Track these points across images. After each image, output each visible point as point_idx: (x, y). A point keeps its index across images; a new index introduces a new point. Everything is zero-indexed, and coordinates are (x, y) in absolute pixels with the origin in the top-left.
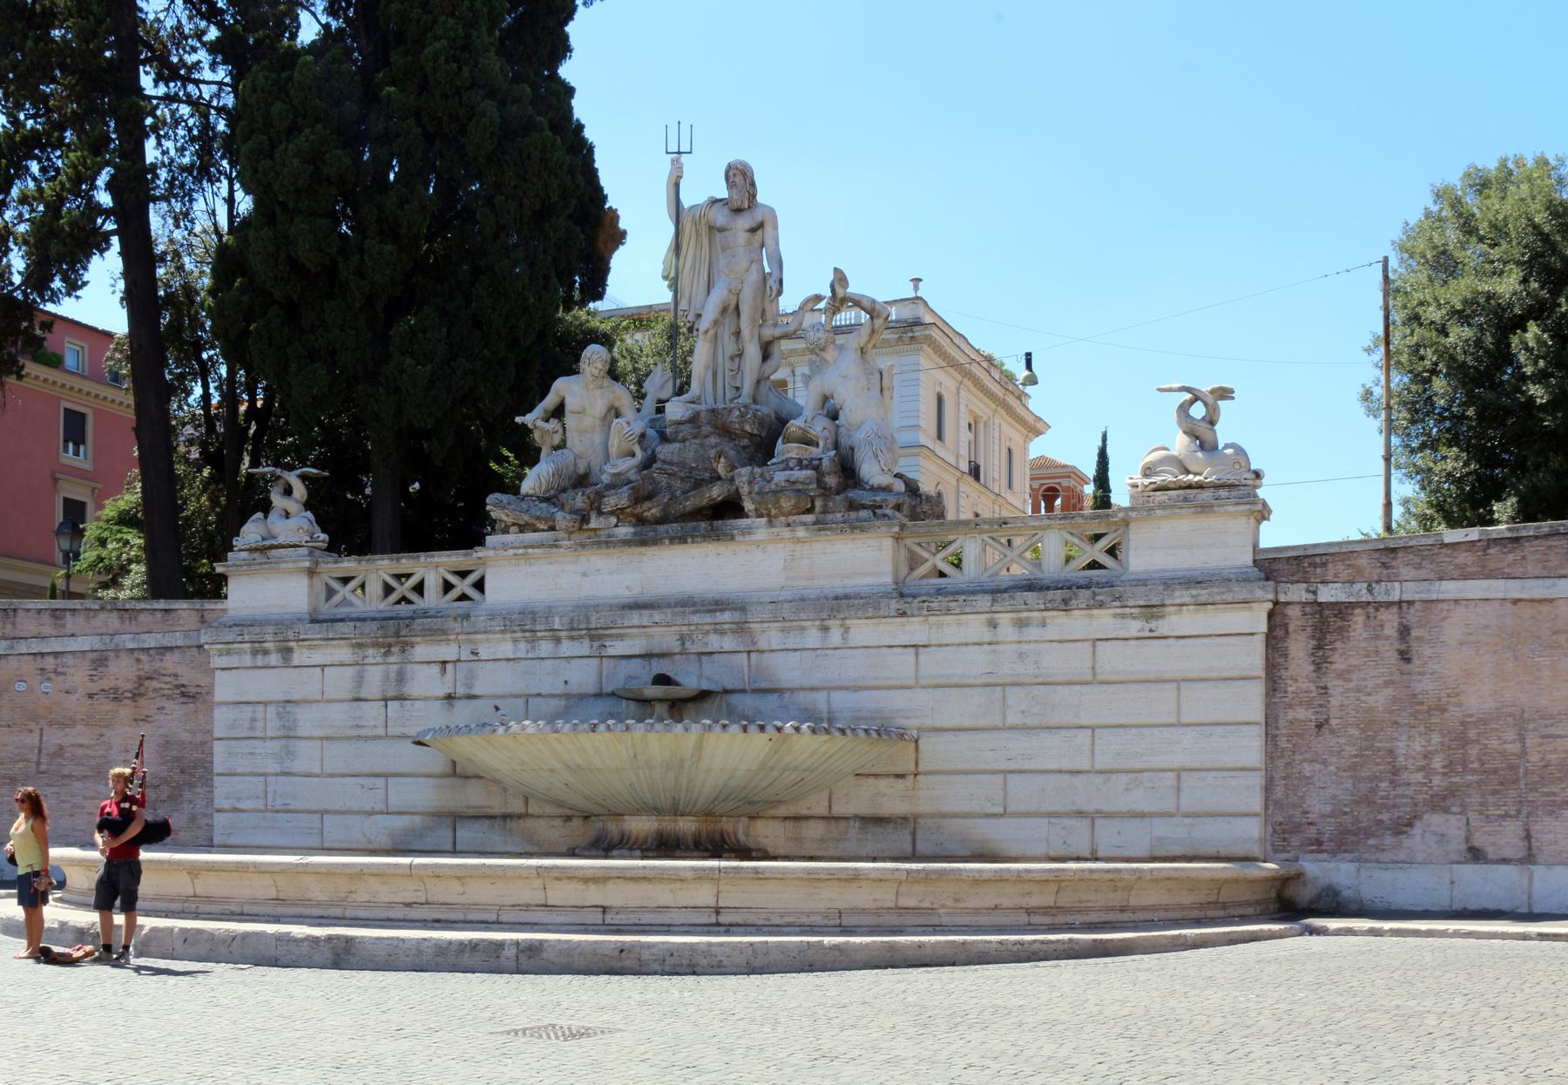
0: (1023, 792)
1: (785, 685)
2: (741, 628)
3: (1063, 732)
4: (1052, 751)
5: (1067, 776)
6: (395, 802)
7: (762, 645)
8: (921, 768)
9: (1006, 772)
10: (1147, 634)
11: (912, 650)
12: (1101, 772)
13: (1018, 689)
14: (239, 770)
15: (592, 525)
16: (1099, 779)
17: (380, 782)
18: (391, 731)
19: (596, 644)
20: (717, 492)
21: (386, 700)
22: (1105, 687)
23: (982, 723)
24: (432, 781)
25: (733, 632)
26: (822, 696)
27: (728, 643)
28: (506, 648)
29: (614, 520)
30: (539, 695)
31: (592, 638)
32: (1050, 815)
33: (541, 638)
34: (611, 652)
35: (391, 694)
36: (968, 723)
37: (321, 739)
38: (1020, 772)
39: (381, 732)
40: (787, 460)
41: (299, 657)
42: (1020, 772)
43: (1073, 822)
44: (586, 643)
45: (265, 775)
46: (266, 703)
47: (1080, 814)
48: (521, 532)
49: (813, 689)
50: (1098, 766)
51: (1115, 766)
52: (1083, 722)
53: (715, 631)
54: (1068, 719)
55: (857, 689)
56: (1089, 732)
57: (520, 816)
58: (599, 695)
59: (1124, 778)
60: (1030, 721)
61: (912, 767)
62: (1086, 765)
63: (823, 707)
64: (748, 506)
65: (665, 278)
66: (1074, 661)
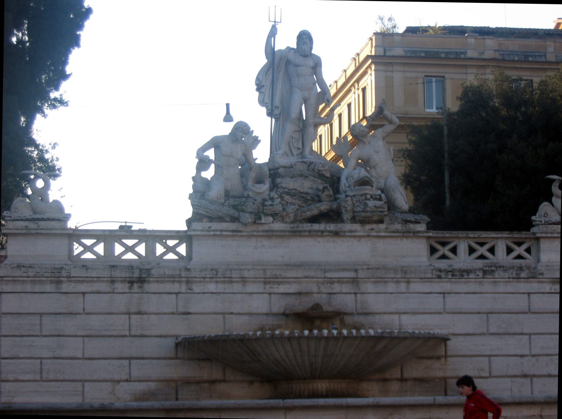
0: (499, 365)
1: (376, 311)
2: (355, 281)
3: (517, 337)
4: (513, 345)
5: (519, 358)
6: (135, 373)
7: (363, 290)
8: (449, 353)
9: (490, 356)
10: (553, 291)
11: (442, 295)
12: (534, 356)
13: (494, 315)
14: (22, 355)
15: (263, 221)
16: (533, 359)
17: (126, 362)
18: (133, 333)
19: (268, 286)
20: (324, 207)
21: (129, 314)
22: (535, 315)
23: (478, 331)
24: (164, 362)
25: (347, 282)
26: (396, 317)
27: (345, 288)
28: (212, 287)
29: (271, 219)
30: (232, 313)
31: (265, 283)
32: (511, 377)
33: (235, 282)
34: (276, 291)
35: (133, 310)
36: (471, 332)
37: (83, 336)
38: (496, 356)
39: (127, 333)
40: (365, 194)
41: (65, 287)
42: (496, 356)
43: (523, 380)
44: (262, 285)
45: (40, 358)
46: (41, 314)
47: (525, 376)
48: (210, 221)
49: (390, 313)
50: (533, 353)
51: (541, 353)
52: (525, 332)
53: (338, 282)
54: (518, 330)
55: (415, 313)
56: (528, 336)
57: (220, 381)
58: (267, 314)
59: (545, 358)
60: (500, 331)
61: (444, 353)
62: (527, 352)
63: (397, 323)
64: (346, 216)
65: (257, 84)
66: (521, 303)
